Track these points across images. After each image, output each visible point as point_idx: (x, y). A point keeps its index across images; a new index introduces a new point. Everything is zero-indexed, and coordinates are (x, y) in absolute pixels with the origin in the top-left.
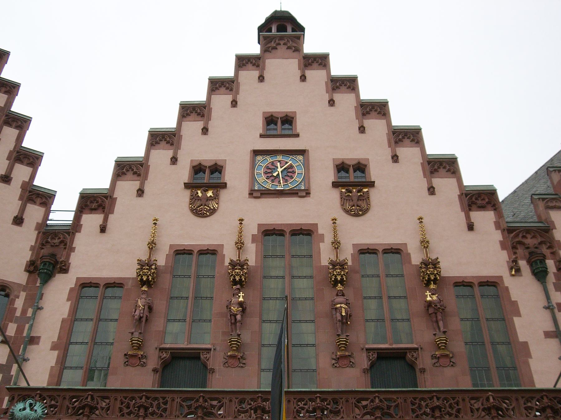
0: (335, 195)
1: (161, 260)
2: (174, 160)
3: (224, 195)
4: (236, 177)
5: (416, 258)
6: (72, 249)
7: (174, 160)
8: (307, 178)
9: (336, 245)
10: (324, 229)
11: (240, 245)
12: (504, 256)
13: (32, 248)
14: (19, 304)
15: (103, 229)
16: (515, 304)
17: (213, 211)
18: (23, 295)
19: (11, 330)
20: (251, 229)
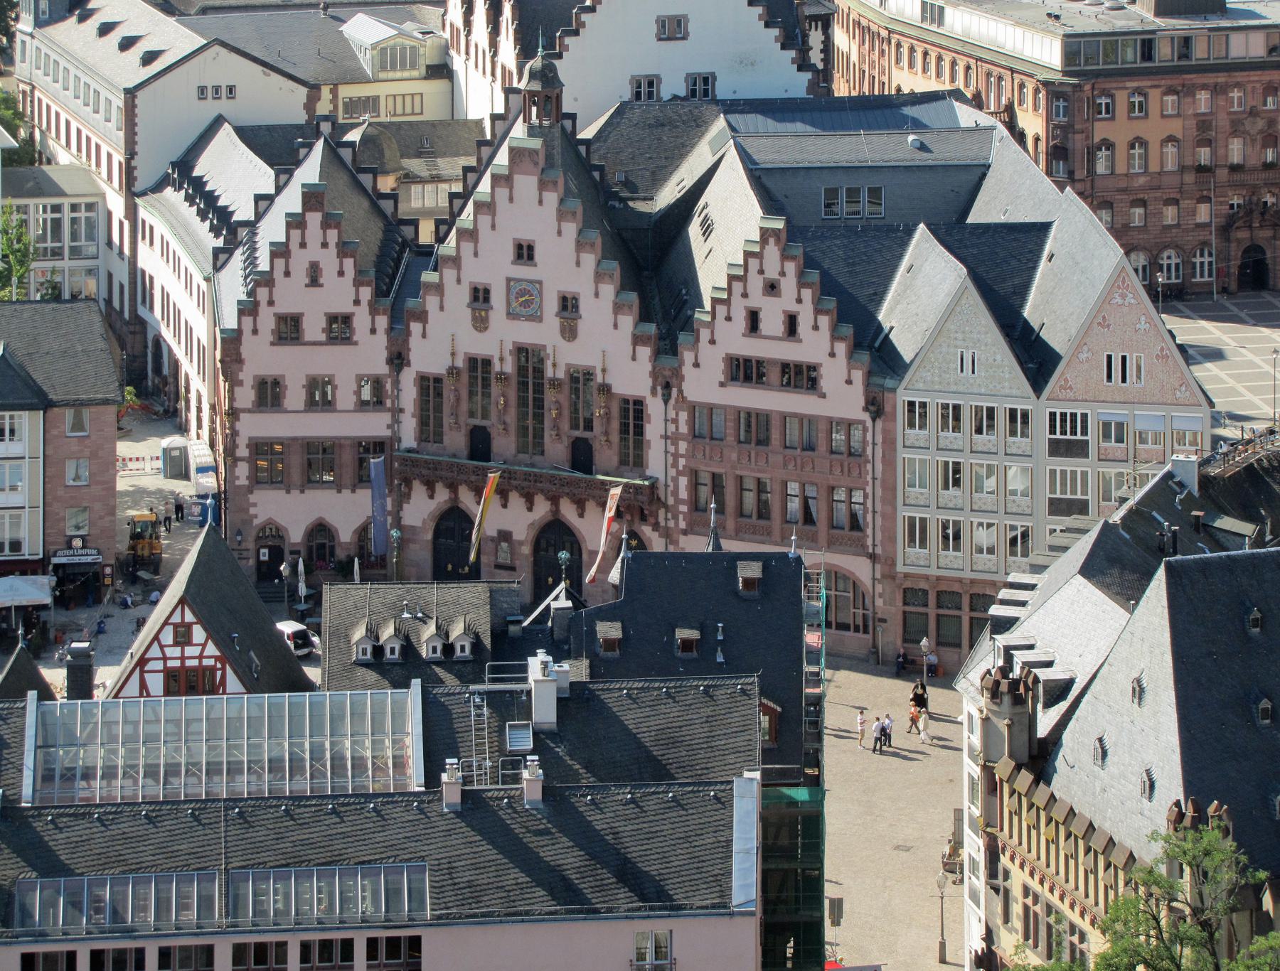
0: (556, 322)
1: (460, 363)
2: (459, 281)
3: (491, 313)
4: (498, 299)
5: (599, 379)
6: (409, 350)
7: (459, 281)
8: (541, 307)
9: (554, 365)
10: (549, 351)
11: (501, 359)
12: (649, 382)
13: (387, 348)
14: (388, 386)
15: (424, 336)
16: (649, 416)
17: (486, 328)
18: (389, 380)
19: (389, 403)
20: (509, 346)
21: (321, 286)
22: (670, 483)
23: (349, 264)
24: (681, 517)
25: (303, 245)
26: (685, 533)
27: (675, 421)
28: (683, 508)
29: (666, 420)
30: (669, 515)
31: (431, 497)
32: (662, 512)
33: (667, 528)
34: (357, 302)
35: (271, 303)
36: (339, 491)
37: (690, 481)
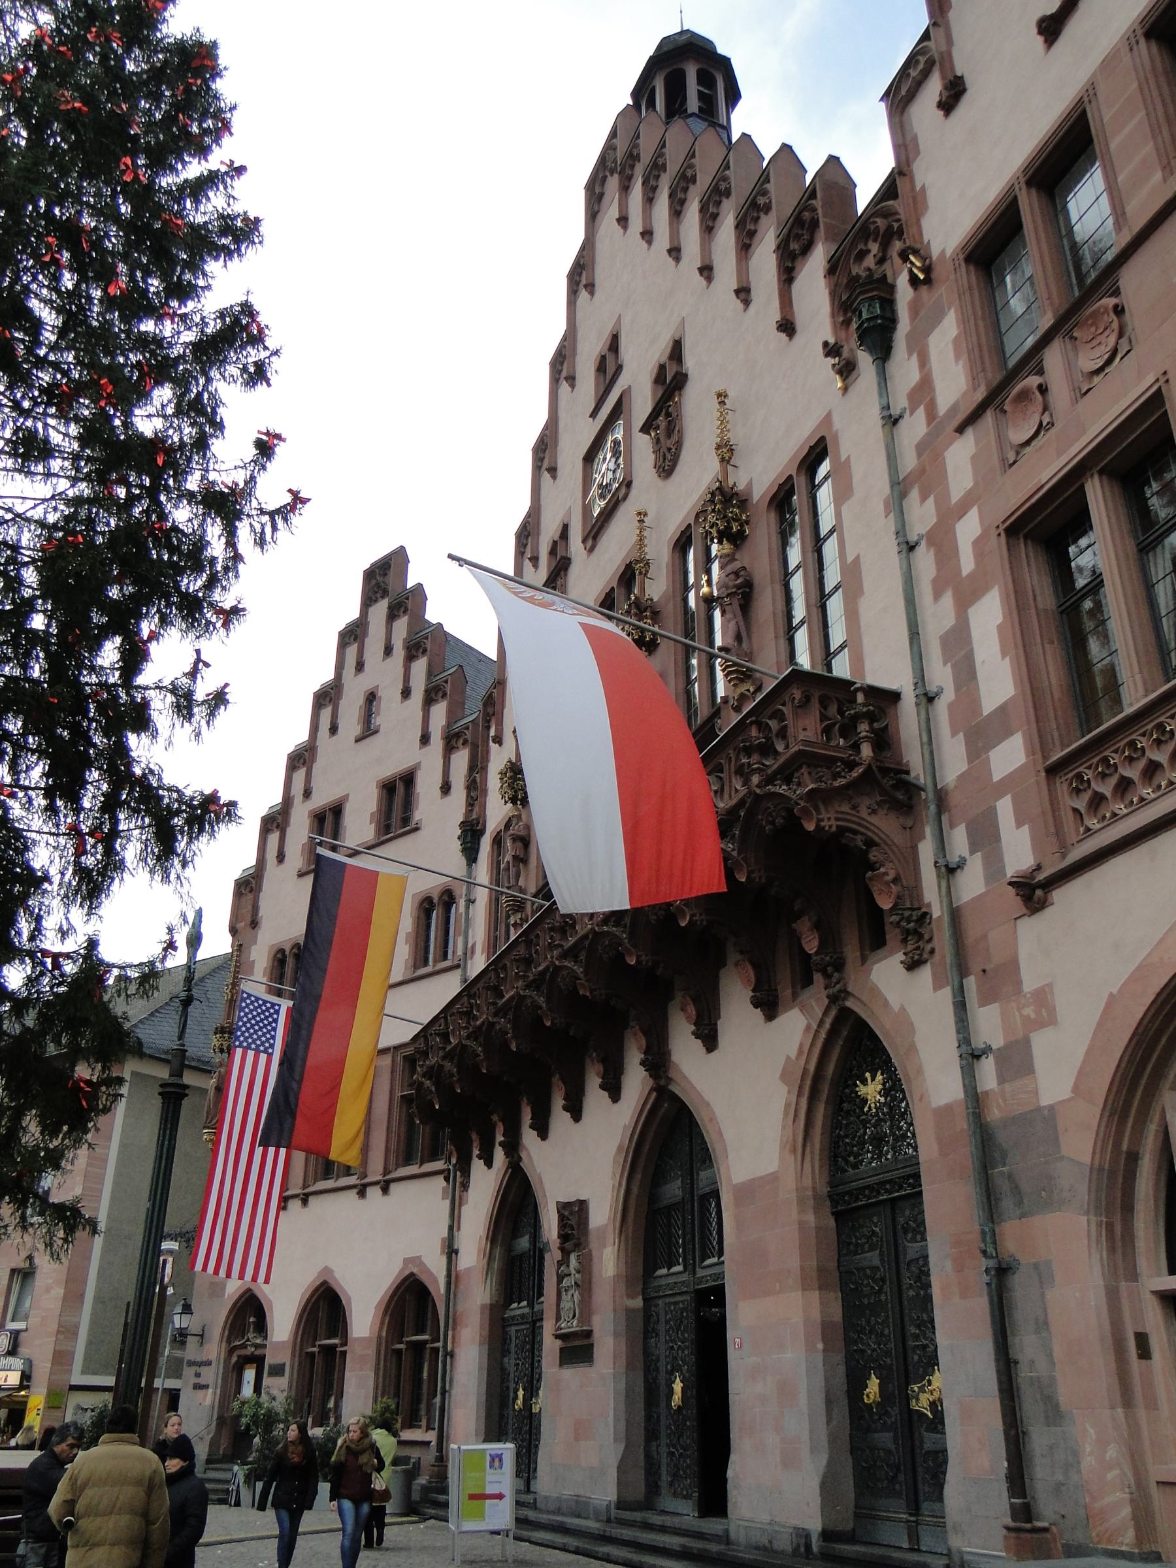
7: (535, 560)
21: (376, 732)
22: (941, 675)
23: (420, 667)
24: (1005, 808)
25: (360, 667)
26: (1033, 892)
27: (924, 391)
28: (1010, 756)
29: (892, 421)
30: (959, 841)
31: (489, 1163)
32: (926, 851)
33: (955, 915)
34: (425, 739)
35: (307, 794)
36: (362, 1193)
37: (1018, 602)
